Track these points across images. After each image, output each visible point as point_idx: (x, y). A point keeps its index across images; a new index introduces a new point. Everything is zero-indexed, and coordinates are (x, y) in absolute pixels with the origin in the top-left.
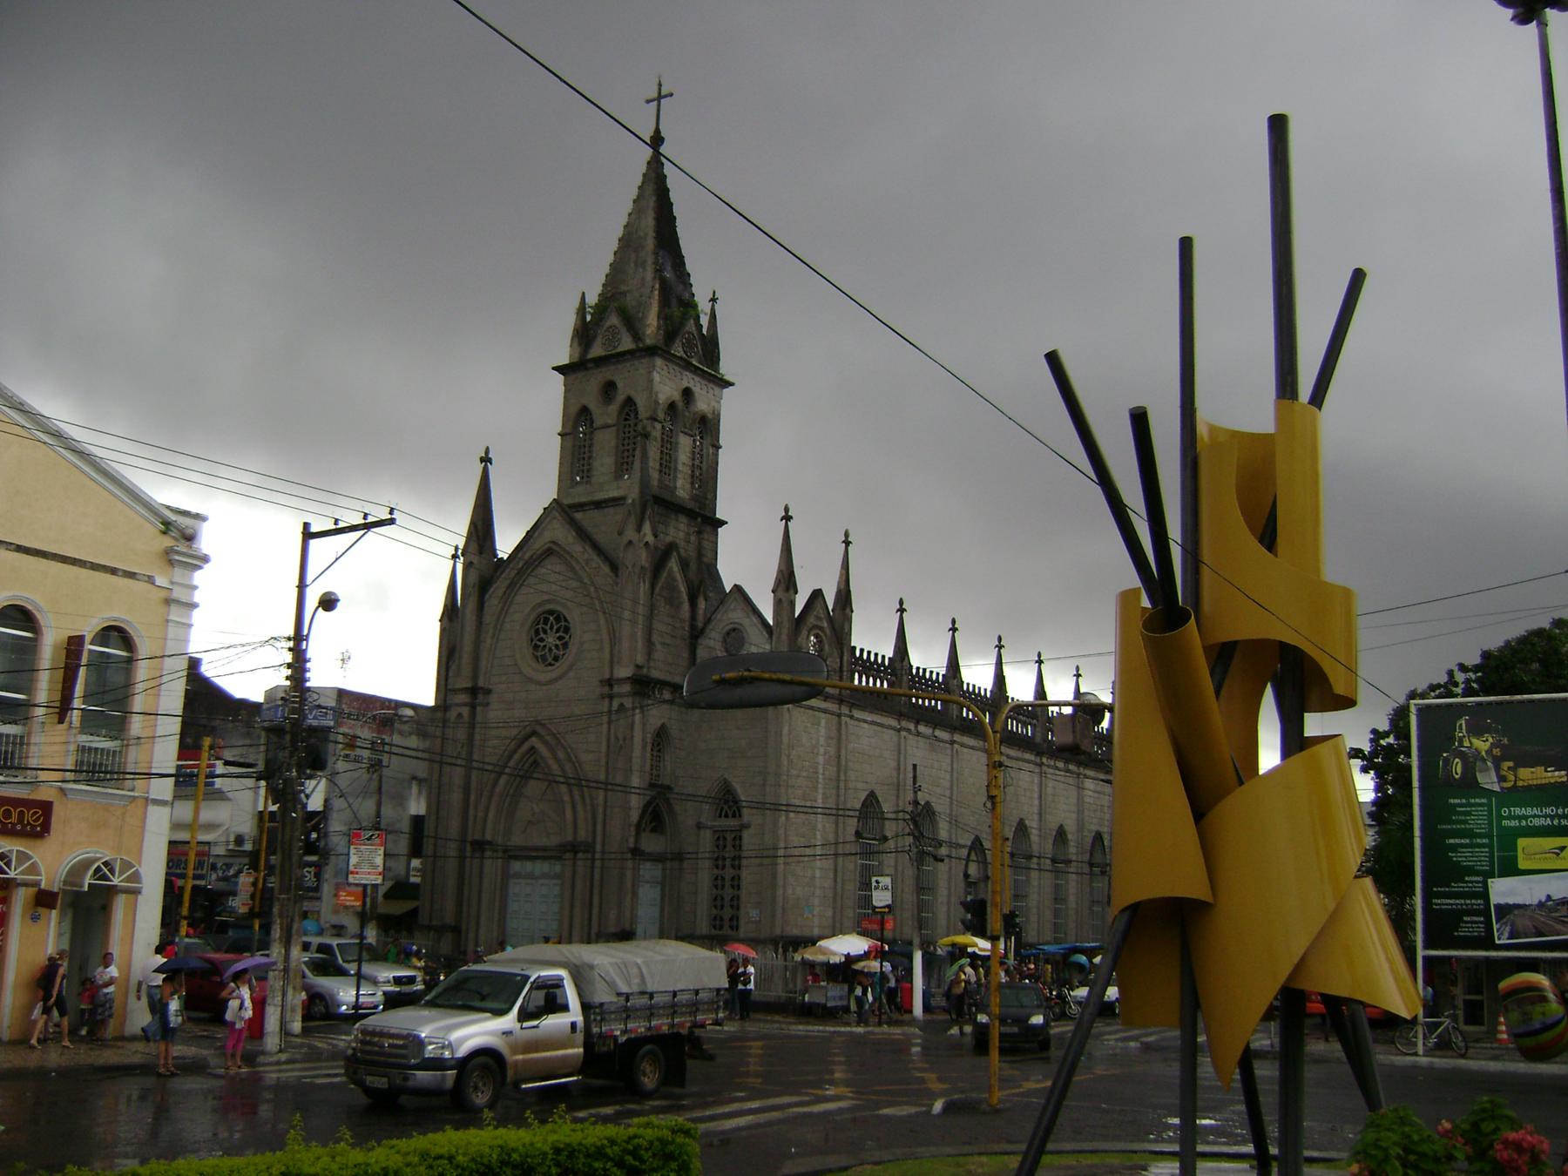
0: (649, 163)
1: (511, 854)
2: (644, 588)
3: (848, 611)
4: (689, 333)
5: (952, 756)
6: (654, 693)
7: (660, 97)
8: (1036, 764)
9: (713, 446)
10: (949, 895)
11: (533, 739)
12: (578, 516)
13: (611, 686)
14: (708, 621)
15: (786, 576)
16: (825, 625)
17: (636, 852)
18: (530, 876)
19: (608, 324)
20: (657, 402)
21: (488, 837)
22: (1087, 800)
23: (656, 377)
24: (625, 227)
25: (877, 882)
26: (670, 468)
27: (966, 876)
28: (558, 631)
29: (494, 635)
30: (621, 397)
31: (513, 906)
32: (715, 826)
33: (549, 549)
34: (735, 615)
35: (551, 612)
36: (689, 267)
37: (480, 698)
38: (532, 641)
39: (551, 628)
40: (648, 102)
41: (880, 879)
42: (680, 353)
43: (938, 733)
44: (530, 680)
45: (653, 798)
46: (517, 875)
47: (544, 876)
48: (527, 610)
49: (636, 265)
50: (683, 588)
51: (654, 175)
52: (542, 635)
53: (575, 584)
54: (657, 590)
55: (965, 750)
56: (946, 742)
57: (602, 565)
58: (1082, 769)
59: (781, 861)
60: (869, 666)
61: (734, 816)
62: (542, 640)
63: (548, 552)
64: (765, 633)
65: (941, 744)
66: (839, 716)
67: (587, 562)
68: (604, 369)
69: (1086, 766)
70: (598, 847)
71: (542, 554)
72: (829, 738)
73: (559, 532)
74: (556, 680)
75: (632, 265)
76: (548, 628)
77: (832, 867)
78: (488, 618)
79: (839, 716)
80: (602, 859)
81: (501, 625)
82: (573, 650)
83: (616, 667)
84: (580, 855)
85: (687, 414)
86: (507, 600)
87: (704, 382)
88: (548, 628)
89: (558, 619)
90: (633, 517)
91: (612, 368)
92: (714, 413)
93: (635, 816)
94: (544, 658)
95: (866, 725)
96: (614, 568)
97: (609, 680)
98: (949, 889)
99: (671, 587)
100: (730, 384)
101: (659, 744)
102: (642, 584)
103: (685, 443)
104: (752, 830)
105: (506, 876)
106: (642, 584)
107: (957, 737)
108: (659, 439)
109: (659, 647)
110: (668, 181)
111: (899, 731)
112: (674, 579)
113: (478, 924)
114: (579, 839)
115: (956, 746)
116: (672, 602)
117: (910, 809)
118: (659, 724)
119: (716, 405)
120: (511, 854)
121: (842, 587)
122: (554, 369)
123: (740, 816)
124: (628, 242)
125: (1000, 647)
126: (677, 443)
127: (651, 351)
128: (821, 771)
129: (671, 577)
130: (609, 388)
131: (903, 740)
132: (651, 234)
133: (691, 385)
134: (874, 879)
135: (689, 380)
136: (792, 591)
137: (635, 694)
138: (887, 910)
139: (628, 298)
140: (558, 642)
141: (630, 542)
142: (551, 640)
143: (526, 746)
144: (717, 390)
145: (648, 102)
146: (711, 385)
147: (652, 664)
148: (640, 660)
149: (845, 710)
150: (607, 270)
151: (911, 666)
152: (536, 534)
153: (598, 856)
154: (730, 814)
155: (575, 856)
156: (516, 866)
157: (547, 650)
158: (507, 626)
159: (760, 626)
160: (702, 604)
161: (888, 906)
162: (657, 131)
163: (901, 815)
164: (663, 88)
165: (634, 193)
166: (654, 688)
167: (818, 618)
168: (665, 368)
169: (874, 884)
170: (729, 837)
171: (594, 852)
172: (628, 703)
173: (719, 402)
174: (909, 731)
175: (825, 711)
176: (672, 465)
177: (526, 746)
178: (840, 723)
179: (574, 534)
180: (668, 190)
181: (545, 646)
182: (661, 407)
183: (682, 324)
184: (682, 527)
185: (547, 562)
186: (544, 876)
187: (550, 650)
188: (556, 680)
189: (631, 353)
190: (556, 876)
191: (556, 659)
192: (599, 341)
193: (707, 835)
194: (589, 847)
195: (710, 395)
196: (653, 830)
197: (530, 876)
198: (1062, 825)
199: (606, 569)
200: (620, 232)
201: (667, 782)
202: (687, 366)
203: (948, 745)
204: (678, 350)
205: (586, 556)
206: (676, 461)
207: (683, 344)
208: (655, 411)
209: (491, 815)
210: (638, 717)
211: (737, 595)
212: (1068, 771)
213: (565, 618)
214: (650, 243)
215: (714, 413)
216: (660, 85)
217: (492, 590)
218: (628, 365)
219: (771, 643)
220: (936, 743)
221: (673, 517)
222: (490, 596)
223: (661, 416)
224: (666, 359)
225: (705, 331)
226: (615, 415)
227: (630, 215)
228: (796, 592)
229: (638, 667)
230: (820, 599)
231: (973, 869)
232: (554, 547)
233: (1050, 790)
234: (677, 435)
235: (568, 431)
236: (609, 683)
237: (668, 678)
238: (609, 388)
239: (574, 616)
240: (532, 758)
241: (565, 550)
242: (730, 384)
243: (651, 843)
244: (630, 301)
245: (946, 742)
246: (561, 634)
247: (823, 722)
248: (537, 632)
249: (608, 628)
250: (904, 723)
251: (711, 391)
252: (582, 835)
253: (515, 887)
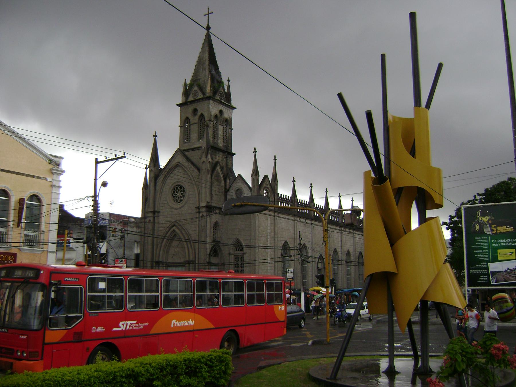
0: (206, 36)
2: (209, 176)
3: (276, 182)
5: (312, 228)
7: (209, 14)
8: (340, 230)
9: (230, 129)
10: (312, 274)
11: (174, 227)
12: (186, 153)
13: (199, 209)
14: (230, 187)
16: (269, 186)
17: (209, 263)
19: (194, 89)
20: (211, 115)
21: (160, 260)
22: (357, 241)
23: (210, 107)
24: (199, 57)
25: (288, 270)
27: (318, 267)
28: (181, 192)
30: (199, 114)
32: (234, 254)
33: (177, 165)
34: (239, 184)
35: (179, 185)
36: (220, 70)
37: (156, 214)
38: (173, 195)
39: (179, 191)
40: (205, 15)
41: (289, 269)
43: (307, 221)
44: (173, 208)
45: (214, 245)
48: (171, 185)
49: (203, 70)
50: (222, 176)
51: (207, 40)
53: (186, 176)
54: (213, 177)
55: (316, 226)
56: (310, 224)
57: (195, 169)
58: (355, 232)
59: (257, 264)
60: (283, 200)
61: (241, 250)
62: (176, 195)
63: (177, 166)
65: (308, 225)
66: (274, 216)
67: (190, 168)
68: (193, 104)
69: (356, 230)
70: (197, 262)
71: (174, 167)
72: (271, 224)
73: (180, 159)
75: (201, 70)
76: (178, 190)
77: (274, 266)
78: (158, 188)
79: (274, 216)
80: (198, 266)
84: (191, 265)
85: (221, 118)
88: (178, 190)
89: (181, 188)
90: (204, 153)
93: (208, 251)
94: (177, 201)
95: (283, 219)
96: (199, 170)
97: (199, 207)
98: (312, 272)
99: (218, 176)
100: (235, 108)
101: (215, 228)
102: (208, 175)
103: (221, 128)
104: (247, 255)
106: (208, 175)
107: (313, 222)
108: (212, 127)
109: (214, 196)
111: (294, 221)
112: (219, 173)
115: (313, 225)
116: (218, 180)
117: (298, 246)
118: (216, 221)
119: (231, 115)
121: (274, 174)
122: (177, 105)
123: (243, 250)
124: (200, 62)
125: (327, 192)
126: (218, 128)
127: (209, 98)
128: (269, 234)
130: (195, 111)
131: (295, 224)
132: (207, 59)
133: (222, 109)
134: (287, 269)
135: (221, 107)
136: (257, 176)
137: (207, 211)
138: (292, 279)
139: (200, 81)
140: (181, 195)
143: (172, 230)
144: (231, 110)
145: (205, 15)
146: (229, 109)
147: (212, 201)
148: (208, 200)
149: (276, 214)
150: (193, 72)
151: (298, 199)
152: (173, 160)
153: (197, 265)
155: (189, 265)
157: (178, 198)
158: (164, 190)
159: (247, 188)
160: (228, 181)
161: (292, 278)
162: (208, 25)
163: (296, 248)
164: (210, 11)
165: (201, 46)
166: (213, 209)
169: (287, 271)
170: (240, 257)
171: (195, 264)
172: (205, 214)
173: (232, 114)
174: (297, 220)
175: (270, 215)
176: (217, 136)
177: (172, 230)
178: (275, 219)
179: (185, 159)
181: (177, 197)
183: (218, 89)
184: (221, 156)
185: (177, 169)
187: (179, 198)
191: (181, 201)
192: (191, 95)
193: (232, 257)
194: (194, 262)
195: (229, 112)
196: (215, 256)
198: (348, 250)
199: (196, 171)
200: (197, 59)
201: (218, 240)
202: (221, 103)
203: (310, 225)
204: (217, 97)
205: (189, 166)
206: (218, 134)
207: (219, 95)
209: (161, 253)
210: (208, 218)
212: (350, 232)
213: (183, 187)
214: (207, 63)
216: (209, 10)
218: (201, 103)
220: (307, 224)
221: (217, 152)
222: (158, 181)
223: (213, 119)
225: (226, 91)
226: (197, 119)
227: (200, 53)
228: (259, 176)
229: (208, 202)
231: (320, 265)
233: (344, 239)
234: (218, 125)
235: (182, 125)
236: (198, 208)
237: (217, 206)
238: (195, 111)
239: (186, 186)
241: (183, 165)
243: (214, 260)
244: (201, 82)
245: (310, 224)
246: (182, 192)
247: (269, 219)
250: (296, 218)
251: (229, 111)
252: (191, 258)
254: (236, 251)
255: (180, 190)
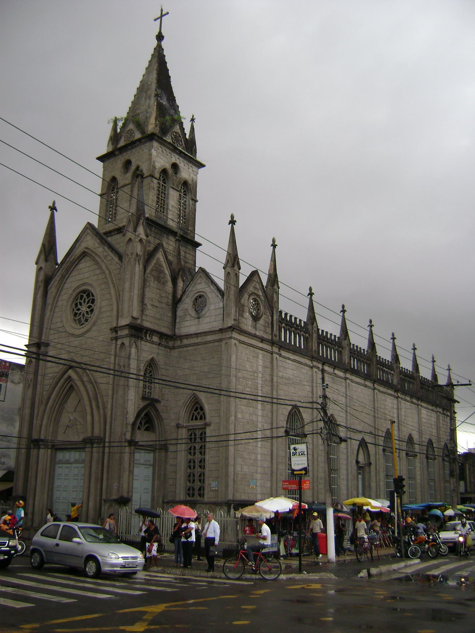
0: (155, 49)
1: (57, 448)
2: (138, 269)
3: (276, 287)
4: (176, 133)
5: (346, 387)
6: (146, 337)
7: (162, 16)
8: (395, 397)
9: (192, 199)
10: (347, 475)
11: (70, 371)
12: (109, 239)
13: (116, 332)
14: (184, 292)
15: (232, 257)
16: (260, 293)
17: (132, 443)
18: (68, 462)
19: (128, 129)
20: (154, 167)
21: (42, 437)
22: (423, 420)
23: (154, 152)
24: (141, 82)
25: (295, 449)
26: (164, 208)
27: (357, 462)
29: (51, 310)
30: (133, 168)
31: (57, 483)
32: (188, 426)
33: (84, 252)
34: (200, 286)
35: (84, 291)
36: (178, 102)
37: (43, 349)
38: (73, 310)
39: (84, 302)
40: (155, 20)
41: (297, 446)
42: (170, 140)
43: (336, 372)
44: (73, 335)
45: (145, 407)
46: (61, 462)
47: (76, 462)
48: (70, 292)
49: (146, 99)
50: (167, 272)
51: (157, 54)
52: (79, 307)
53: (98, 271)
54: (148, 271)
55: (354, 384)
56: (342, 378)
57: (114, 258)
58: (419, 402)
59: (231, 443)
61: (201, 418)
62: (79, 309)
63: (84, 254)
64: (219, 296)
65: (339, 379)
66: (272, 353)
67: (105, 257)
68: (125, 154)
69: (422, 401)
70: (107, 440)
71: (79, 258)
72: (265, 367)
73: (91, 242)
74: (87, 331)
75: (144, 99)
76: (82, 301)
77: (269, 453)
78: (50, 301)
79: (272, 353)
80: (109, 447)
81: (56, 303)
82: (96, 312)
83: (120, 319)
84: (95, 445)
85: (175, 178)
86: (60, 289)
87: (185, 162)
88: (82, 301)
89: (88, 296)
90: (132, 223)
91: (129, 152)
92: (192, 181)
93: (131, 418)
94: (80, 321)
95: (290, 362)
96: (120, 257)
97: (115, 327)
98: (347, 470)
99: (159, 270)
100: (203, 166)
101: (151, 372)
102: (137, 265)
103: (173, 197)
104: (212, 427)
105: (53, 462)
106: (137, 265)
107: (348, 375)
108: (156, 188)
109: (149, 307)
110: (166, 58)
111: (312, 368)
112: (161, 266)
113: (35, 494)
114: (95, 435)
115: (348, 381)
116: (159, 278)
117: (320, 401)
118: (150, 357)
119: (194, 177)
120: (57, 448)
121: (272, 272)
123: (205, 419)
124: (142, 89)
125: (371, 326)
126: (168, 194)
127: (151, 137)
128: (260, 388)
129: (158, 264)
131: (314, 374)
132: (155, 81)
133: (178, 162)
134: (292, 447)
135: (175, 158)
136: (236, 267)
137: (131, 336)
138: (303, 472)
139: (140, 116)
140: (88, 310)
141: (130, 240)
142: (84, 309)
143: (66, 376)
144: (195, 168)
145: (155, 20)
146: (190, 165)
147: (144, 318)
148: (135, 314)
149: (275, 349)
150: (130, 105)
151: (318, 329)
152: (77, 246)
153: (107, 444)
154: (199, 418)
155: (92, 445)
156: (60, 455)
157: (81, 316)
158: (60, 303)
159: (216, 291)
160: (180, 284)
161: (305, 469)
162: (160, 33)
163: (315, 406)
164: (163, 11)
165: (146, 64)
166: (146, 333)
167: (255, 288)
168: (160, 148)
169: (292, 451)
170: (198, 433)
171: (105, 442)
172: (126, 341)
173: (196, 176)
174: (318, 368)
175: (262, 349)
176: (165, 207)
177: (66, 376)
178: (272, 358)
179: (98, 241)
180: (166, 63)
181: (80, 313)
182: (157, 170)
183: (172, 127)
184: (171, 243)
185: (82, 261)
186: (76, 462)
187: (83, 315)
188: (87, 331)
189: (139, 140)
190: (83, 462)
191: (86, 320)
192: (123, 139)
193: (183, 433)
194: (101, 440)
195: (191, 170)
196: (147, 429)
197: (68, 462)
198: (410, 434)
199: (116, 259)
200: (138, 85)
201: (156, 397)
202: (175, 150)
203: (343, 380)
204: (168, 139)
205: (105, 253)
206: (168, 204)
207: (172, 138)
208: (153, 172)
209: (45, 422)
210: (133, 350)
211: (201, 274)
212: (412, 402)
214: (154, 86)
215: (192, 181)
216: (162, 10)
217: (52, 283)
218: (138, 148)
219: (223, 302)
220: (336, 378)
221: (165, 236)
222: (51, 287)
223: (157, 175)
224: (161, 143)
225: (187, 137)
226: (130, 178)
227: (144, 76)
228: (240, 269)
229: (133, 318)
230: (256, 276)
231: (361, 459)
232: (87, 251)
233: (403, 413)
234: (168, 189)
235: (104, 192)
236: (115, 330)
237: (156, 328)
238: (128, 163)
239: (97, 292)
240: (70, 384)
241: (92, 251)
242: (203, 166)
243: (142, 437)
244: (141, 118)
245: (342, 378)
246: (90, 304)
247: (261, 356)
248: (76, 305)
249: (116, 294)
250: (315, 363)
251: (190, 168)
252: (97, 432)
253: (60, 470)
254: (192, 420)
255: (87, 301)
